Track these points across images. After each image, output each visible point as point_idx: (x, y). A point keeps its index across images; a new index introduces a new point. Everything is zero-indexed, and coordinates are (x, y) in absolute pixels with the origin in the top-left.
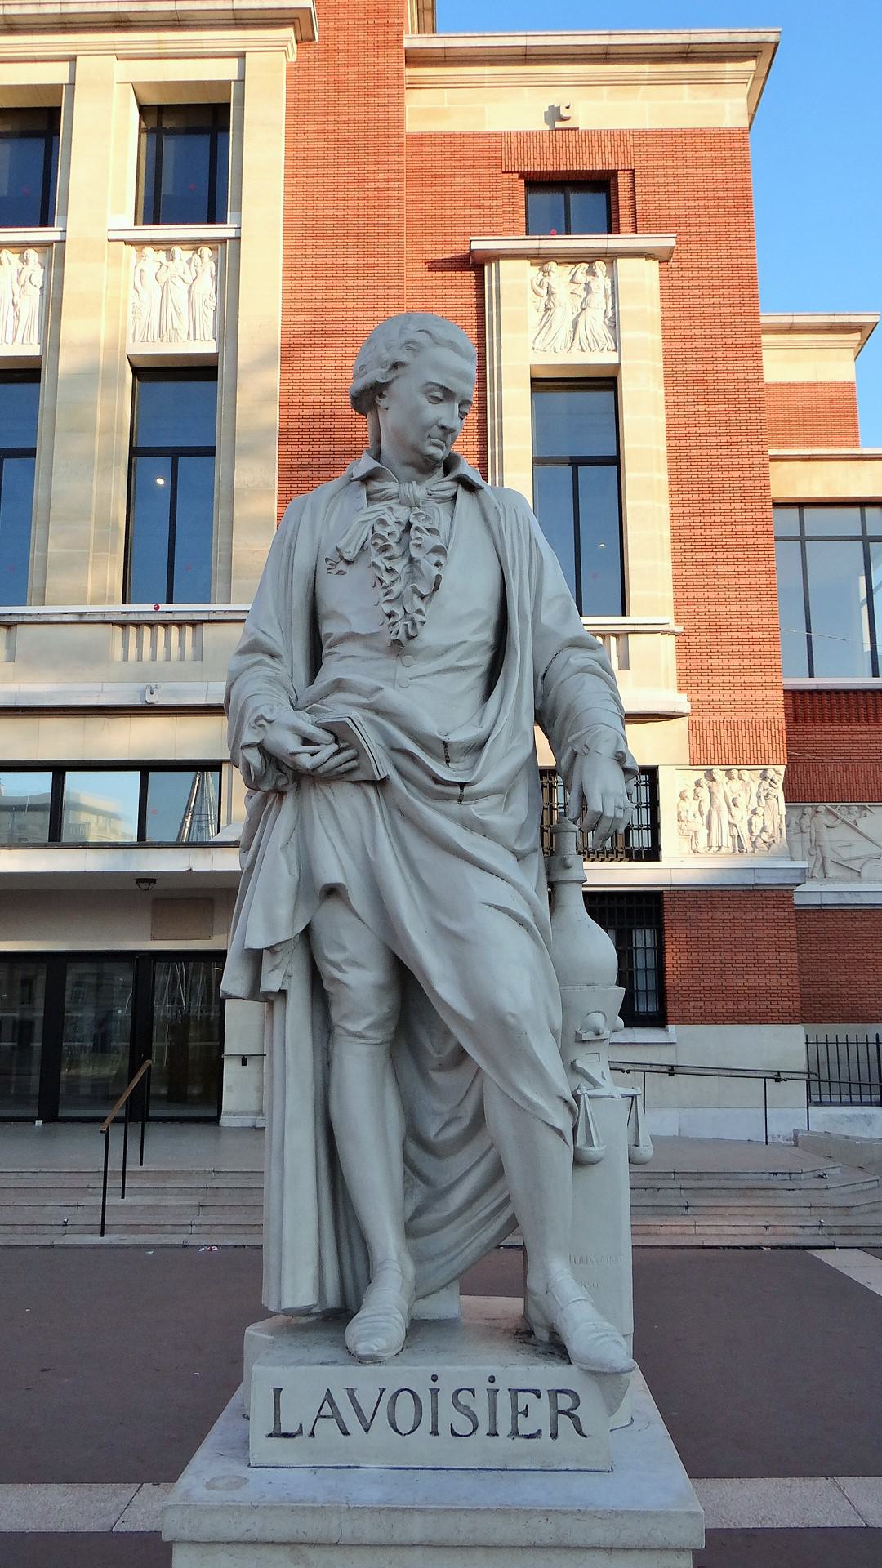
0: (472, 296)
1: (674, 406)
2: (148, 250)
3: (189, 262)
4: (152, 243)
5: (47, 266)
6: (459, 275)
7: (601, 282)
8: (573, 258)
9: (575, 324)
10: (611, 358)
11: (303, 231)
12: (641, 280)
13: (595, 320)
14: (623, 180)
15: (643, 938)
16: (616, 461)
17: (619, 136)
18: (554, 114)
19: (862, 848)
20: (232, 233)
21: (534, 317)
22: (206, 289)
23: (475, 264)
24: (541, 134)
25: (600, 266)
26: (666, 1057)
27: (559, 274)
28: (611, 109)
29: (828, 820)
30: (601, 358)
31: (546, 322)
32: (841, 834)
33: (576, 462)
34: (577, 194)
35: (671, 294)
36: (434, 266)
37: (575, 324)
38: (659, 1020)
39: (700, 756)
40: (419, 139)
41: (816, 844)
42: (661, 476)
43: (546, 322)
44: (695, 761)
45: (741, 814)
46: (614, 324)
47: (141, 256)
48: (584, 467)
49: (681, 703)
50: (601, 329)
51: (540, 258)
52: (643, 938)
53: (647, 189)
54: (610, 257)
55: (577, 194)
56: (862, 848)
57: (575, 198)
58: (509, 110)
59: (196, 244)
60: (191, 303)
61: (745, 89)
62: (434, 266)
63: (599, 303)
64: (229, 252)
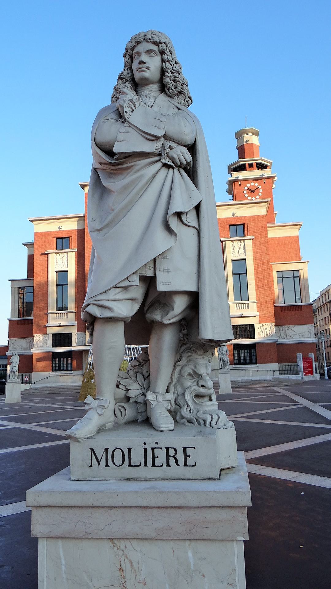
1: (255, 265)
7: (242, 244)
8: (238, 240)
10: (244, 257)
12: (249, 243)
13: (242, 251)
14: (246, 225)
15: (253, 351)
16: (246, 273)
17: (244, 217)
18: (233, 214)
19: (293, 333)
21: (232, 250)
25: (242, 241)
26: (257, 369)
29: (287, 328)
30: (244, 257)
31: (234, 252)
32: (290, 331)
33: (240, 274)
34: (239, 228)
35: (254, 245)
38: (256, 363)
39: (261, 322)
41: (285, 333)
42: (253, 277)
43: (234, 252)
44: (260, 323)
45: (268, 331)
46: (245, 251)
48: (240, 274)
49: (257, 314)
52: (253, 351)
53: (250, 227)
54: (244, 240)
55: (239, 228)
56: (293, 333)
61: (266, 207)
63: (242, 247)
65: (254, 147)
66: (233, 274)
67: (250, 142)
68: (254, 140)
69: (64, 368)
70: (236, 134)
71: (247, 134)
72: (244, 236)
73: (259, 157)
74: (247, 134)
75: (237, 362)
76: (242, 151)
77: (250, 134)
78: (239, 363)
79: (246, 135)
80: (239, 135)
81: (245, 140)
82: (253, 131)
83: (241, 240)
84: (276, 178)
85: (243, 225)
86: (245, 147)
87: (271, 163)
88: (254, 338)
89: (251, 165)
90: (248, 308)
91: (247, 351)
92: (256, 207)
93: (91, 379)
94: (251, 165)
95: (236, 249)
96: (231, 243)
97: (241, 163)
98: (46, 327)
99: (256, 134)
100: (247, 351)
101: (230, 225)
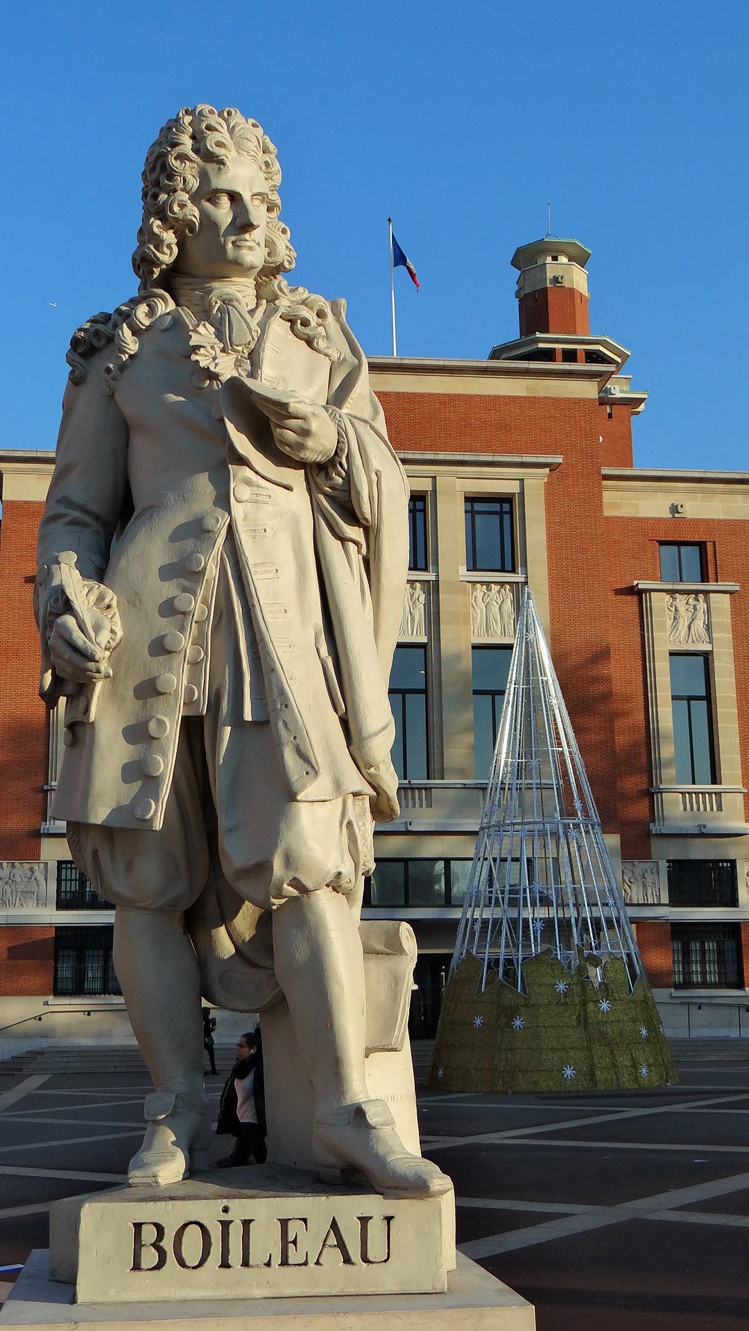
0: (636, 609)
2: (478, 586)
3: (499, 592)
4: (482, 583)
5: (428, 593)
6: (629, 598)
7: (702, 606)
9: (689, 627)
10: (708, 647)
11: (558, 582)
12: (721, 603)
13: (700, 624)
18: (674, 509)
20: (523, 580)
21: (669, 622)
22: (508, 606)
23: (638, 593)
24: (667, 519)
27: (680, 600)
28: (703, 507)
33: (689, 699)
35: (736, 611)
36: (618, 592)
37: (689, 627)
40: (607, 518)
43: (675, 626)
46: (708, 628)
47: (474, 589)
50: (703, 632)
51: (672, 592)
53: (725, 555)
54: (706, 593)
57: (683, 549)
58: (652, 505)
59: (502, 584)
60: (501, 616)
62: (618, 592)
64: (518, 590)
65: (577, 300)
66: (674, 698)
67: (566, 284)
68: (578, 279)
69: (98, 985)
70: (519, 251)
71: (555, 259)
72: (704, 578)
73: (575, 333)
74: (555, 259)
75: (679, 978)
76: (537, 308)
77: (563, 259)
78: (687, 984)
79: (549, 259)
80: (528, 258)
81: (550, 275)
82: (573, 251)
83: (696, 592)
84: (642, 407)
85: (702, 545)
86: (551, 297)
87: (625, 357)
88: (733, 902)
89: (570, 356)
90: (720, 809)
91: (710, 945)
92: (703, 492)
93: (511, 1017)
94: (570, 356)
95: (681, 621)
96: (667, 597)
97: (541, 345)
98: (37, 835)
99: (581, 259)
100: (710, 945)
101: (662, 543)
